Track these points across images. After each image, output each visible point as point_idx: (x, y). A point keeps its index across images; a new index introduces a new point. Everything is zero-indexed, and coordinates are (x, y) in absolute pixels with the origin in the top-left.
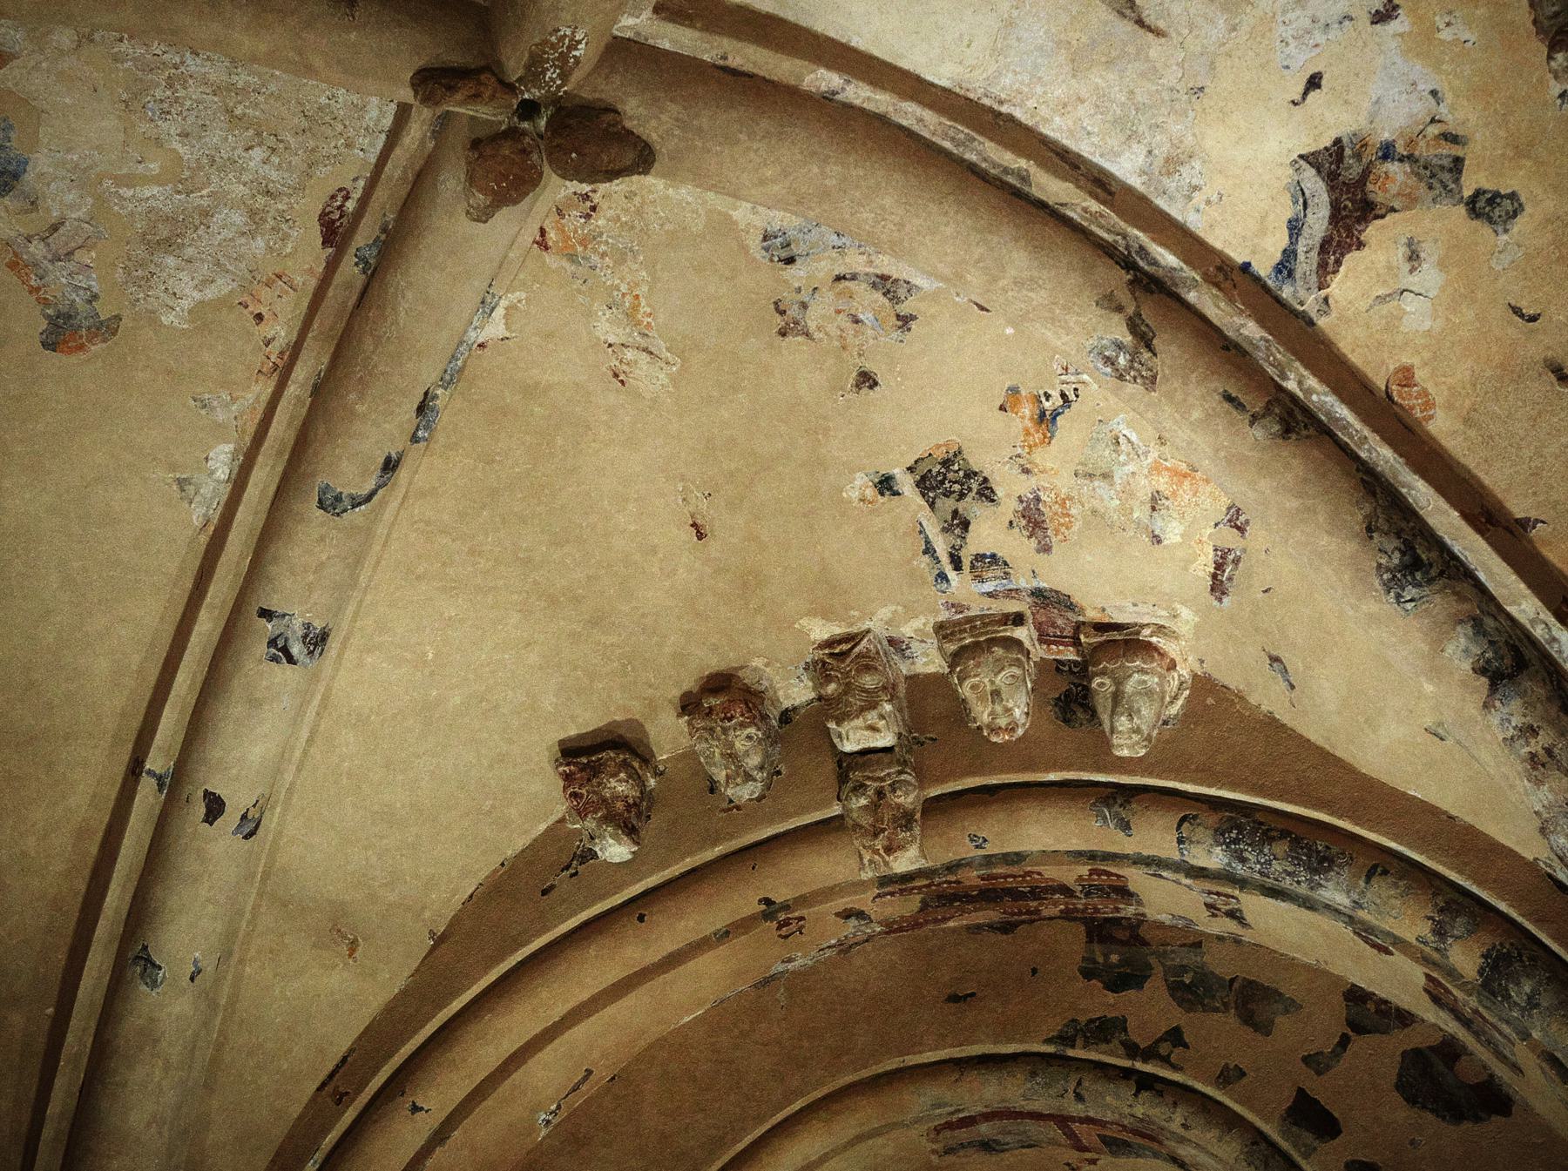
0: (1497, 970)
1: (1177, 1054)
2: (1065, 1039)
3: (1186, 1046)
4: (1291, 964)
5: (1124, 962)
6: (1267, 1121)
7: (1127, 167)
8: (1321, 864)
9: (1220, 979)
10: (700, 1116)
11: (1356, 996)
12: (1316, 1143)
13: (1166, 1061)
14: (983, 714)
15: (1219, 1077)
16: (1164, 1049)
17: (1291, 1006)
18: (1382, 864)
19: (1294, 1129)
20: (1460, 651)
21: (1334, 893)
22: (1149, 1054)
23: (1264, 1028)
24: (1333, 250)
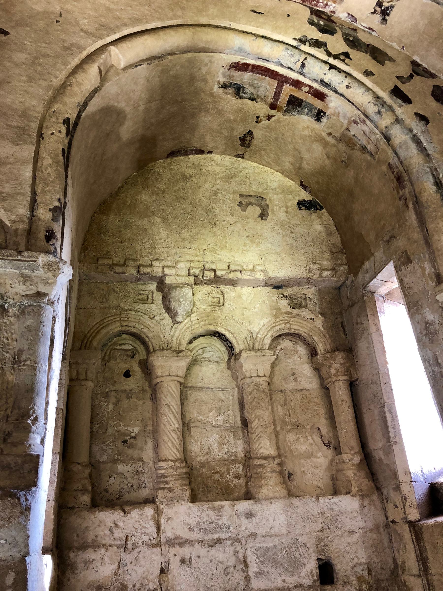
1: (347, 60)
2: (302, 41)
3: (351, 59)
5: (325, 25)
6: (384, 90)
9: (364, 44)
10: (129, 8)
11: (414, 63)
12: (403, 104)
13: (343, 61)
15: (365, 72)
16: (342, 57)
17: (391, 59)
19: (394, 97)
22: (336, 57)
23: (382, 63)
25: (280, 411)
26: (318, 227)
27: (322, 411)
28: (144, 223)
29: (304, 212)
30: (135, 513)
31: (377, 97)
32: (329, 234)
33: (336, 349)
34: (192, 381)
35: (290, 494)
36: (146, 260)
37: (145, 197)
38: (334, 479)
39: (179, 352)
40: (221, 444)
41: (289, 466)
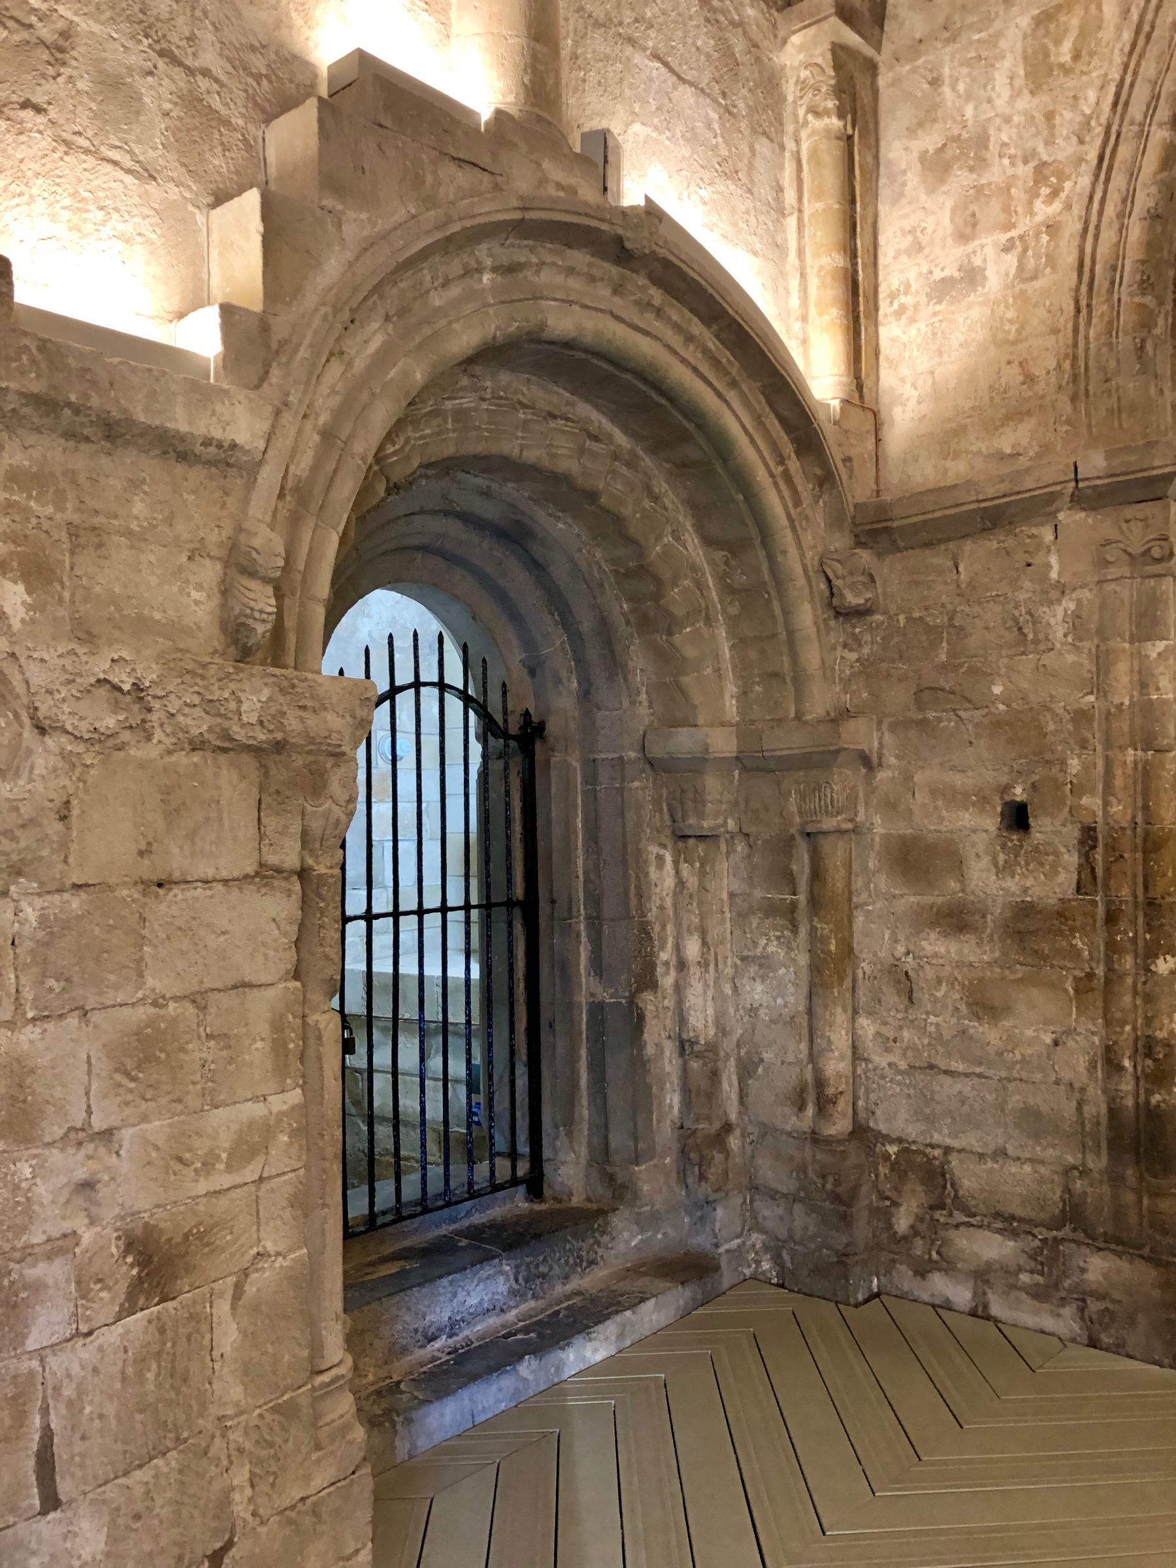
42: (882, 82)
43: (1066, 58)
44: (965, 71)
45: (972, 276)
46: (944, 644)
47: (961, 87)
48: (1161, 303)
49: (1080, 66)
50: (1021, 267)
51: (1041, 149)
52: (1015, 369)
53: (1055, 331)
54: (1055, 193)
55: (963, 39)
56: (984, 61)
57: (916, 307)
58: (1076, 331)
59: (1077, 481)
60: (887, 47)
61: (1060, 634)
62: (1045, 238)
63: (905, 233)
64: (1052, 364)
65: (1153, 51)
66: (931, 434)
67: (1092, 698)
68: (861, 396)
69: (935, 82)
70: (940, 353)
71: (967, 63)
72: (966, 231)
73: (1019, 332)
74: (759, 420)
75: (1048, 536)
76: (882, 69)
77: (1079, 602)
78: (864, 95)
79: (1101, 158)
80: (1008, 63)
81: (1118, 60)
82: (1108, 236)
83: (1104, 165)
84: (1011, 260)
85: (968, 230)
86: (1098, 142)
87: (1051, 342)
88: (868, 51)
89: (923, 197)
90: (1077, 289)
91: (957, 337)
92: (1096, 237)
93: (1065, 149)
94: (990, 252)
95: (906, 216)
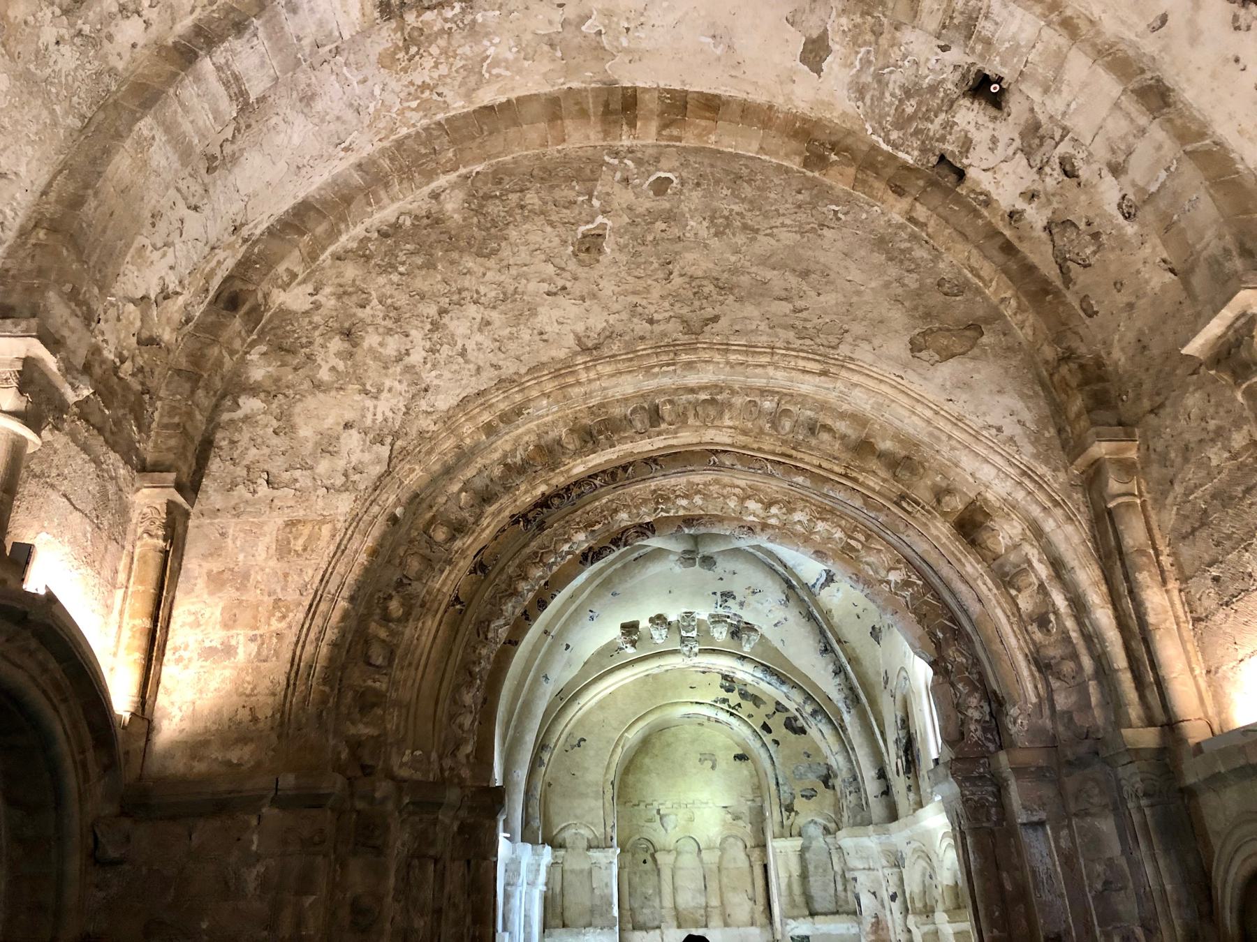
0: (814, 714)
4: (765, 693)
7: (790, 564)
8: (783, 683)
11: (778, 703)
14: (716, 635)
17: (764, 703)
18: (795, 686)
20: (831, 667)
21: (784, 688)
23: (758, 707)
24: (823, 586)
25: (725, 880)
26: (746, 772)
27: (749, 880)
28: (647, 778)
29: (738, 762)
30: (651, 933)
31: (755, 731)
32: (752, 776)
33: (758, 846)
34: (679, 864)
35: (726, 925)
36: (649, 801)
37: (647, 761)
38: (752, 918)
39: (669, 851)
40: (693, 898)
41: (728, 911)
42: (191, 523)
43: (299, 548)
44: (242, 535)
45: (228, 650)
46: (172, 890)
47: (238, 543)
48: (332, 688)
49: (306, 555)
50: (259, 653)
51: (279, 590)
52: (247, 711)
53: (274, 694)
54: (284, 617)
55: (244, 518)
56: (253, 533)
57: (190, 660)
58: (286, 696)
59: (277, 789)
60: (197, 507)
61: (251, 889)
62: (275, 640)
63: (190, 613)
64: (269, 714)
65: (344, 560)
66: (186, 742)
67: (266, 933)
68: (143, 710)
69: (223, 535)
70: (201, 692)
71: (245, 532)
72: (230, 622)
73: (253, 690)
74: (75, 726)
75: (254, 822)
76: (192, 516)
77: (267, 868)
78: (179, 529)
79: (311, 606)
80: (267, 539)
81: (326, 559)
82: (309, 649)
83: (312, 610)
84: (253, 647)
85: (231, 623)
86: (311, 597)
87: (270, 700)
88: (187, 506)
89: (206, 596)
90: (289, 674)
91: (214, 685)
92: (303, 647)
93: (291, 596)
94: (241, 638)
95: (193, 603)
